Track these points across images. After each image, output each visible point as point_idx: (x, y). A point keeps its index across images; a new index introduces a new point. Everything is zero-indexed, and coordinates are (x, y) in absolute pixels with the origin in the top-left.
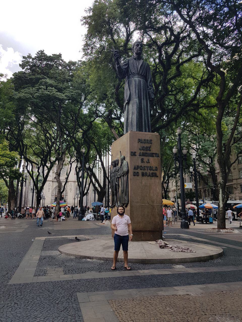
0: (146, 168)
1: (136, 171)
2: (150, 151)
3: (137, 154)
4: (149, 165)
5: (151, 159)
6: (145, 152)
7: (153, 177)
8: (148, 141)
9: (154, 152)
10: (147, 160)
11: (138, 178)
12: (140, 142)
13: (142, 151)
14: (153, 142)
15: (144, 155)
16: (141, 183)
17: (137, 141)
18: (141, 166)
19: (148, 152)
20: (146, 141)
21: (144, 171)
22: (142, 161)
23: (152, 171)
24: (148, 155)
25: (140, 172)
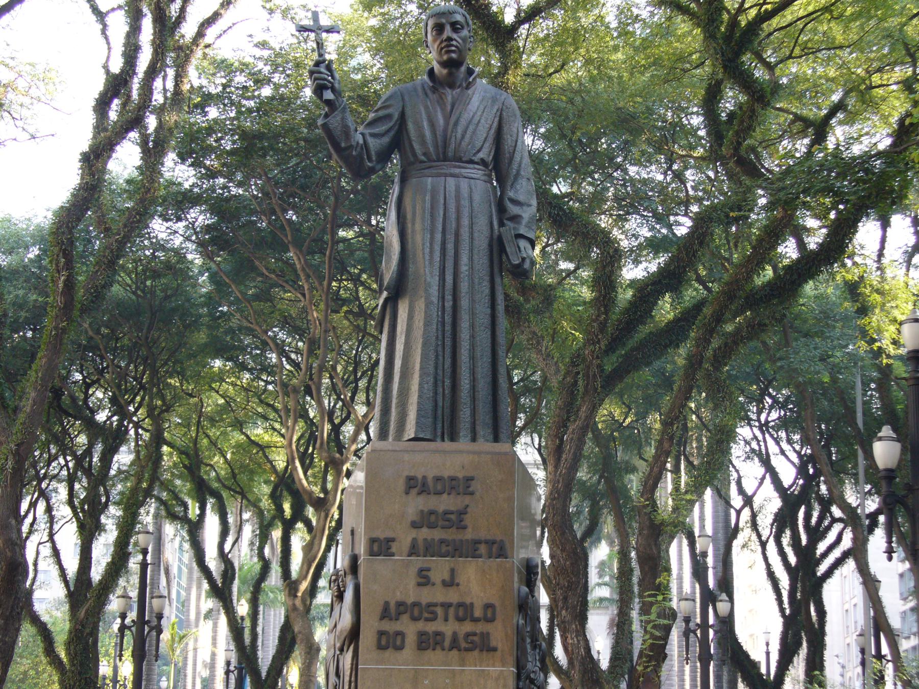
0: (439, 611)
4: (453, 596)
6: (437, 534)
9: (483, 535)
10: (446, 576)
12: (414, 492)
13: (425, 533)
14: (475, 486)
15: (430, 549)
18: (415, 604)
21: (430, 624)
22: (424, 579)
23: (468, 627)
25: (410, 629)
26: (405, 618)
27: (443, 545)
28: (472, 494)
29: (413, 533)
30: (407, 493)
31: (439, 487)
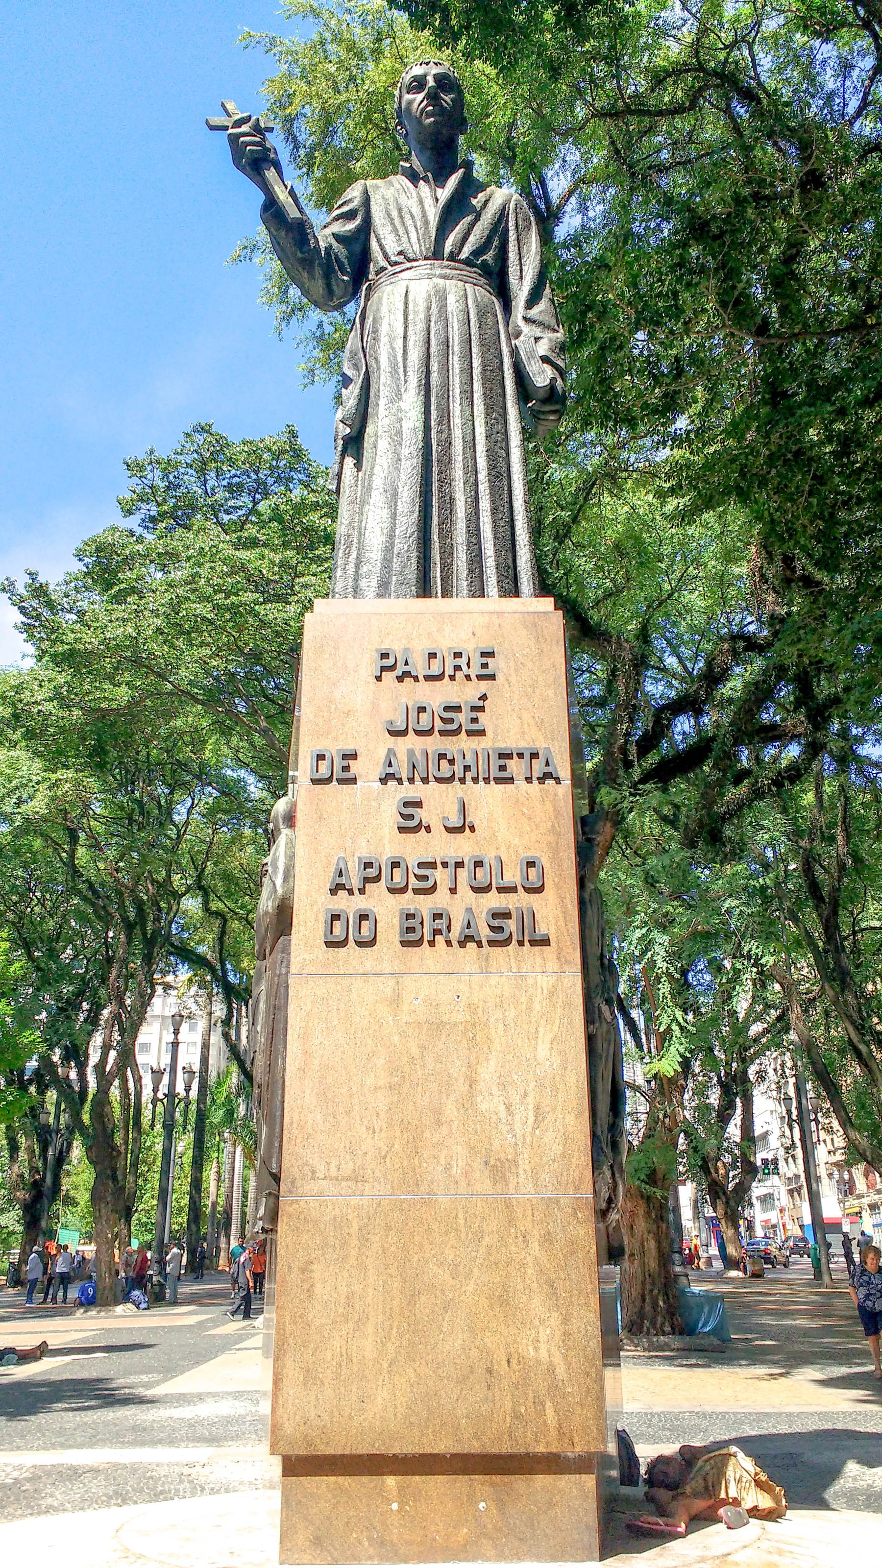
0: (440, 876)
2: (482, 733)
3: (367, 769)
4: (462, 847)
5: (487, 801)
6: (435, 744)
7: (506, 942)
8: (462, 662)
11: (367, 958)
16: (395, 1001)
17: (370, 665)
19: (464, 743)
20: (443, 668)
22: (410, 823)
23: (494, 901)
24: (458, 769)
25: (386, 908)
26: (378, 890)
27: (444, 763)
28: (492, 677)
29: (391, 741)
30: (379, 679)
31: (435, 670)
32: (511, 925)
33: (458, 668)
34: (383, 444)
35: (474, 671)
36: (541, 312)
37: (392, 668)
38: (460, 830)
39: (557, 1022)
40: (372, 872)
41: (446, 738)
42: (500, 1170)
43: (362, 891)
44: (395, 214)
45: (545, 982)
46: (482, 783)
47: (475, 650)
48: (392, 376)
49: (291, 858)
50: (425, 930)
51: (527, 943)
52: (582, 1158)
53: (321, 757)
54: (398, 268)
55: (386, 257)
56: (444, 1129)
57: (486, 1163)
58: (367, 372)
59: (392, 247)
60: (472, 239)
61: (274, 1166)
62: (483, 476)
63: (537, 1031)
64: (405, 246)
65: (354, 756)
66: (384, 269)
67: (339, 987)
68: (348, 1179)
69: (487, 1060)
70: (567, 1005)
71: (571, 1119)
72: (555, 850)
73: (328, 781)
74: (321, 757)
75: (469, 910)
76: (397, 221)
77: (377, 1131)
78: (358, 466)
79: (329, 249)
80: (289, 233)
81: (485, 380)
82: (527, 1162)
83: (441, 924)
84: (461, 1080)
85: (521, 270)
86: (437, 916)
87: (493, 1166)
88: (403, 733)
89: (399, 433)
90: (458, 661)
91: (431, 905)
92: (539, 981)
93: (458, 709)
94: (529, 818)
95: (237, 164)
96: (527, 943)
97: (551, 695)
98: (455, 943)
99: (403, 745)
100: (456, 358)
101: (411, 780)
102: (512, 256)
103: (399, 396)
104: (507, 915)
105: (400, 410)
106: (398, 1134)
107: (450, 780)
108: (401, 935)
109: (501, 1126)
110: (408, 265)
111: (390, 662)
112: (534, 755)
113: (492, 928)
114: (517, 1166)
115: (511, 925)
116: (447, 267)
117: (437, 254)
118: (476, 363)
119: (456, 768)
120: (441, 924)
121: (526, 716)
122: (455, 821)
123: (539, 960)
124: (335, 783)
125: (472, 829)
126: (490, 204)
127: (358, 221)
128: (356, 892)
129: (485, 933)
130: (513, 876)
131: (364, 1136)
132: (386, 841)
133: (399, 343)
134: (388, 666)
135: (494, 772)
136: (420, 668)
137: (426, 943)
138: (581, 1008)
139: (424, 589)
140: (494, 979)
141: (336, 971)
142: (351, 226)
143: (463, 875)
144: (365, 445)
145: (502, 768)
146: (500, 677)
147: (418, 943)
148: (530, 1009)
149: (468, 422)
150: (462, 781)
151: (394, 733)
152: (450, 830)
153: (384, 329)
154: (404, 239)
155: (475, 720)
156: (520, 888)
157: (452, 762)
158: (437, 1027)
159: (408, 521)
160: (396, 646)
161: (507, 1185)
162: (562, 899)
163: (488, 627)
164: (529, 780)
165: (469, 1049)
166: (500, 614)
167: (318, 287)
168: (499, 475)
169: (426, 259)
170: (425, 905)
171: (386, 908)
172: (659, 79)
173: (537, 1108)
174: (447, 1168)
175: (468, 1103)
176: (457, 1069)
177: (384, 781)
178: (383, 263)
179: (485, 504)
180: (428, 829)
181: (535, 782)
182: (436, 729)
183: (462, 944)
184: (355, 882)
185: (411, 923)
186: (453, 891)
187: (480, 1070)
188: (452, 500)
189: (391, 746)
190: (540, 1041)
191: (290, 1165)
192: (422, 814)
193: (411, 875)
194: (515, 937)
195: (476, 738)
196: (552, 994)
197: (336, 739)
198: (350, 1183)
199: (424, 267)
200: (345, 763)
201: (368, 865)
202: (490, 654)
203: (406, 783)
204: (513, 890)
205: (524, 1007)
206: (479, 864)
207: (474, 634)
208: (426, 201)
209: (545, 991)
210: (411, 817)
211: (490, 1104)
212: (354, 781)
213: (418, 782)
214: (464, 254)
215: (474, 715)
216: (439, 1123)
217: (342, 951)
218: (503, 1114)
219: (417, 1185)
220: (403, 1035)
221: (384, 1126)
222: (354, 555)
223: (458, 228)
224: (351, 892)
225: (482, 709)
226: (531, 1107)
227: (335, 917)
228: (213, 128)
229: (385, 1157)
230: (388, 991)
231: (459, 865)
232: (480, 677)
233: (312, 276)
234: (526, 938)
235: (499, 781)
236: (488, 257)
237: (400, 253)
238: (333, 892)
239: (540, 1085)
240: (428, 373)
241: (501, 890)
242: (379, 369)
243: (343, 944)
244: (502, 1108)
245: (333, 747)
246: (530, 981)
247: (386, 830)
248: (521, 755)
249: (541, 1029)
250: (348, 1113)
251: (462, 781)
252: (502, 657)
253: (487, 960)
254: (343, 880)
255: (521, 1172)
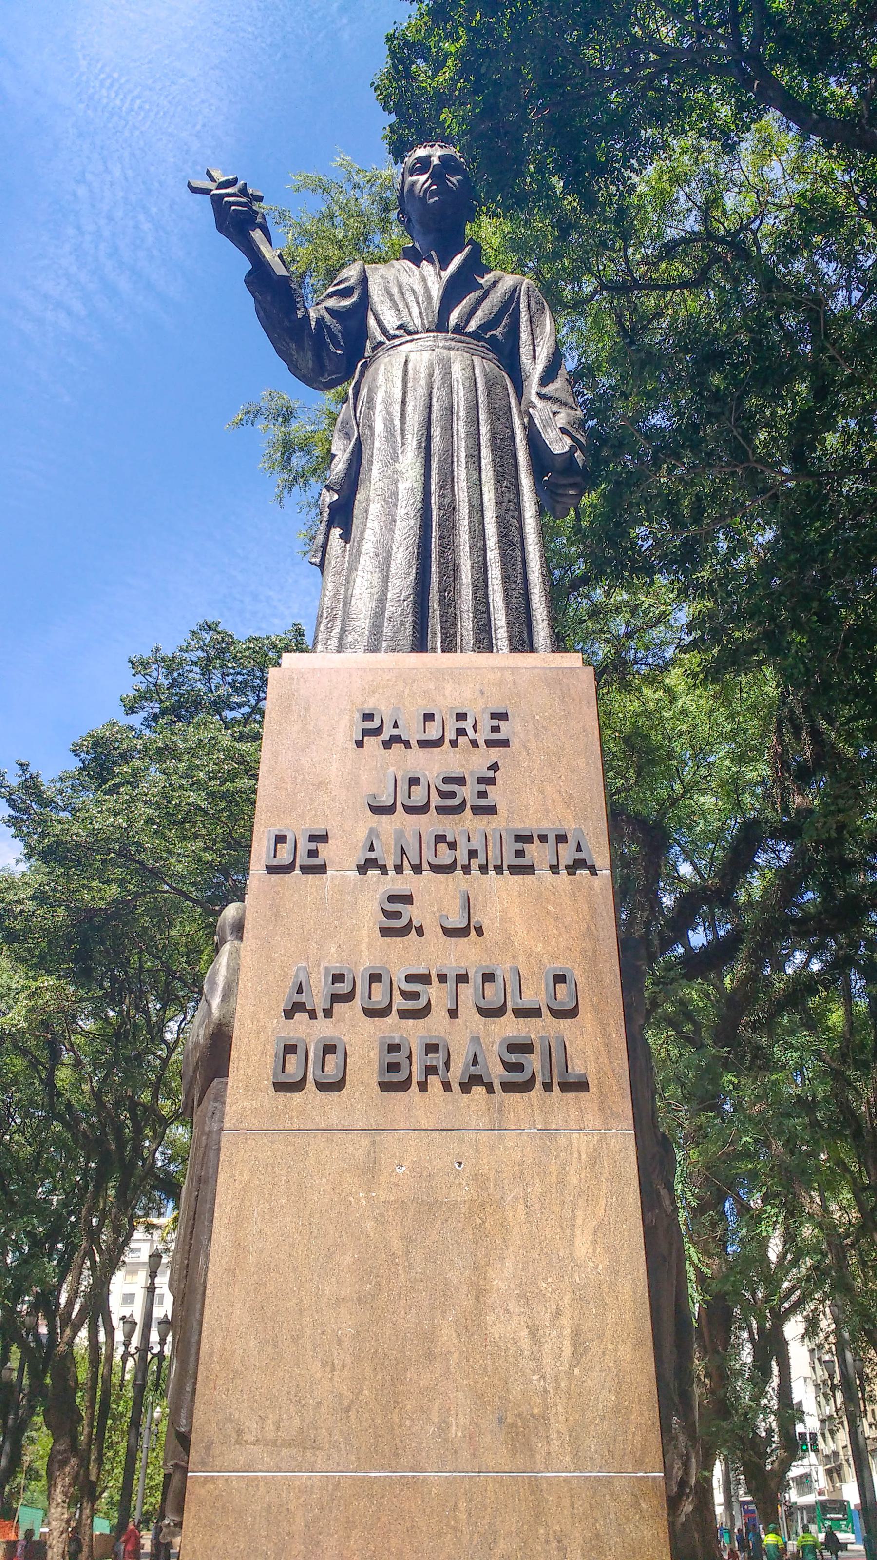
0: (435, 993)
1: (311, 1032)
2: (491, 810)
3: (342, 855)
6: (430, 824)
7: (526, 1086)
8: (468, 725)
16: (370, 1171)
17: (348, 727)
19: (469, 823)
22: (396, 924)
23: (510, 1028)
24: (462, 856)
25: (361, 1037)
28: (505, 743)
30: (360, 744)
31: (433, 733)
32: (534, 1062)
33: (461, 732)
34: (375, 508)
35: (483, 735)
36: (557, 389)
37: (378, 731)
38: (463, 932)
39: (603, 1202)
40: (343, 988)
41: (448, 808)
42: (521, 1431)
43: (328, 1013)
44: (395, 290)
45: (582, 1143)
46: (492, 873)
47: (484, 710)
48: (388, 441)
49: (234, 971)
50: (414, 1068)
51: (556, 1088)
52: (644, 1413)
53: (280, 839)
54: (397, 342)
55: (384, 331)
56: (438, 1366)
57: (501, 1421)
58: (359, 441)
59: (391, 321)
60: (479, 313)
61: (184, 1421)
62: (492, 542)
63: (573, 1217)
64: (406, 319)
65: (323, 838)
66: (381, 344)
67: (290, 1149)
68: (290, 1444)
69: (502, 1259)
70: (616, 1177)
71: (626, 1352)
72: (592, 960)
73: (287, 869)
74: (280, 839)
75: (476, 1040)
76: (397, 297)
77: (338, 1367)
78: (346, 536)
79: (320, 321)
80: (274, 295)
81: (495, 448)
82: (562, 1418)
83: (437, 1060)
84: (464, 1289)
85: (534, 351)
86: (431, 1048)
87: (513, 1425)
88: (389, 810)
89: (395, 494)
90: (461, 724)
91: (422, 1033)
92: (575, 1142)
93: (461, 781)
94: (557, 919)
95: (221, 226)
96: (556, 1088)
97: (582, 765)
98: (456, 1087)
99: (387, 824)
100: (461, 423)
101: (399, 869)
102: (524, 336)
103: (395, 458)
104: (526, 1048)
105: (396, 472)
106: (369, 1372)
107: (449, 869)
108: (381, 1073)
109: (523, 1363)
110: (409, 338)
111: (376, 723)
112: (562, 838)
113: (510, 1067)
114: (547, 1426)
115: (534, 1062)
116: (452, 339)
117: (440, 325)
118: (484, 429)
119: (458, 853)
120: (437, 1060)
121: (549, 789)
122: (457, 921)
123: (573, 1113)
124: (297, 871)
125: (480, 931)
126: (500, 285)
127: (354, 298)
128: (320, 1014)
129: (496, 1072)
130: (535, 994)
131: (319, 1375)
132: (364, 947)
133: (397, 407)
134: (370, 728)
135: (509, 859)
136: (413, 731)
137: (414, 1087)
138: (636, 1183)
139: (420, 645)
140: (511, 1139)
141: (288, 1125)
142: (347, 302)
143: (467, 992)
144: (355, 512)
145: (519, 854)
146: (515, 743)
147: (404, 1086)
148: (562, 1181)
149: (475, 489)
150: (466, 869)
151: (378, 810)
152: (449, 932)
153: (379, 397)
154: (405, 313)
155: (483, 795)
156: (545, 1011)
157: (453, 846)
158: (430, 1208)
159: (401, 582)
160: (384, 709)
161: (532, 1456)
162: (604, 1026)
163: (500, 683)
164: (554, 869)
165: (475, 1242)
166: (514, 670)
167: (308, 361)
168: (512, 544)
169: (428, 331)
170: (414, 1033)
171: (361, 1037)
172: (669, 250)
173: (576, 1334)
174: (443, 1428)
175: (472, 1326)
176: (457, 1272)
177: (362, 869)
178: (381, 338)
179: (495, 573)
180: (420, 932)
181: (563, 872)
182: (433, 805)
183: (465, 1088)
184: (319, 1002)
185: (394, 1058)
186: (453, 1013)
187: (491, 1274)
188: (456, 569)
189: (374, 825)
190: (578, 1232)
191: (204, 1421)
192: (412, 913)
193: (396, 992)
194: (539, 1079)
195: (486, 818)
196: (594, 1160)
197: (302, 816)
198: (294, 1451)
199: (426, 340)
200: (313, 846)
201: (338, 978)
202: (503, 716)
203: (392, 872)
204: (535, 1013)
205: (554, 1179)
206: (488, 977)
207: (482, 693)
208: (431, 279)
209: (584, 1157)
210: (398, 915)
211: (506, 1326)
212: (321, 869)
213: (408, 872)
214: (472, 326)
215: (482, 788)
216: (430, 1356)
217: (297, 1098)
218: (525, 1343)
219: (396, 1455)
220: (380, 1220)
221: (348, 1360)
222: (337, 630)
223: (465, 301)
224: (313, 1015)
225: (492, 781)
226: (567, 1332)
227: (290, 1049)
228: (194, 190)
229: (348, 1410)
230: (360, 1154)
231: (462, 978)
232: (490, 743)
233: (300, 347)
234: (555, 1081)
235: (515, 870)
236: (498, 332)
237: (400, 327)
238: (289, 1014)
239: (580, 1300)
240: (429, 438)
241: (520, 1013)
242: (373, 434)
243: (298, 1086)
244: (524, 1333)
245: (299, 828)
246: (563, 1141)
247: (365, 932)
248: (543, 838)
249: (580, 1214)
250: (295, 1339)
251: (466, 869)
252: (518, 719)
253: (500, 1111)
254: (303, 998)
255: (554, 1436)
